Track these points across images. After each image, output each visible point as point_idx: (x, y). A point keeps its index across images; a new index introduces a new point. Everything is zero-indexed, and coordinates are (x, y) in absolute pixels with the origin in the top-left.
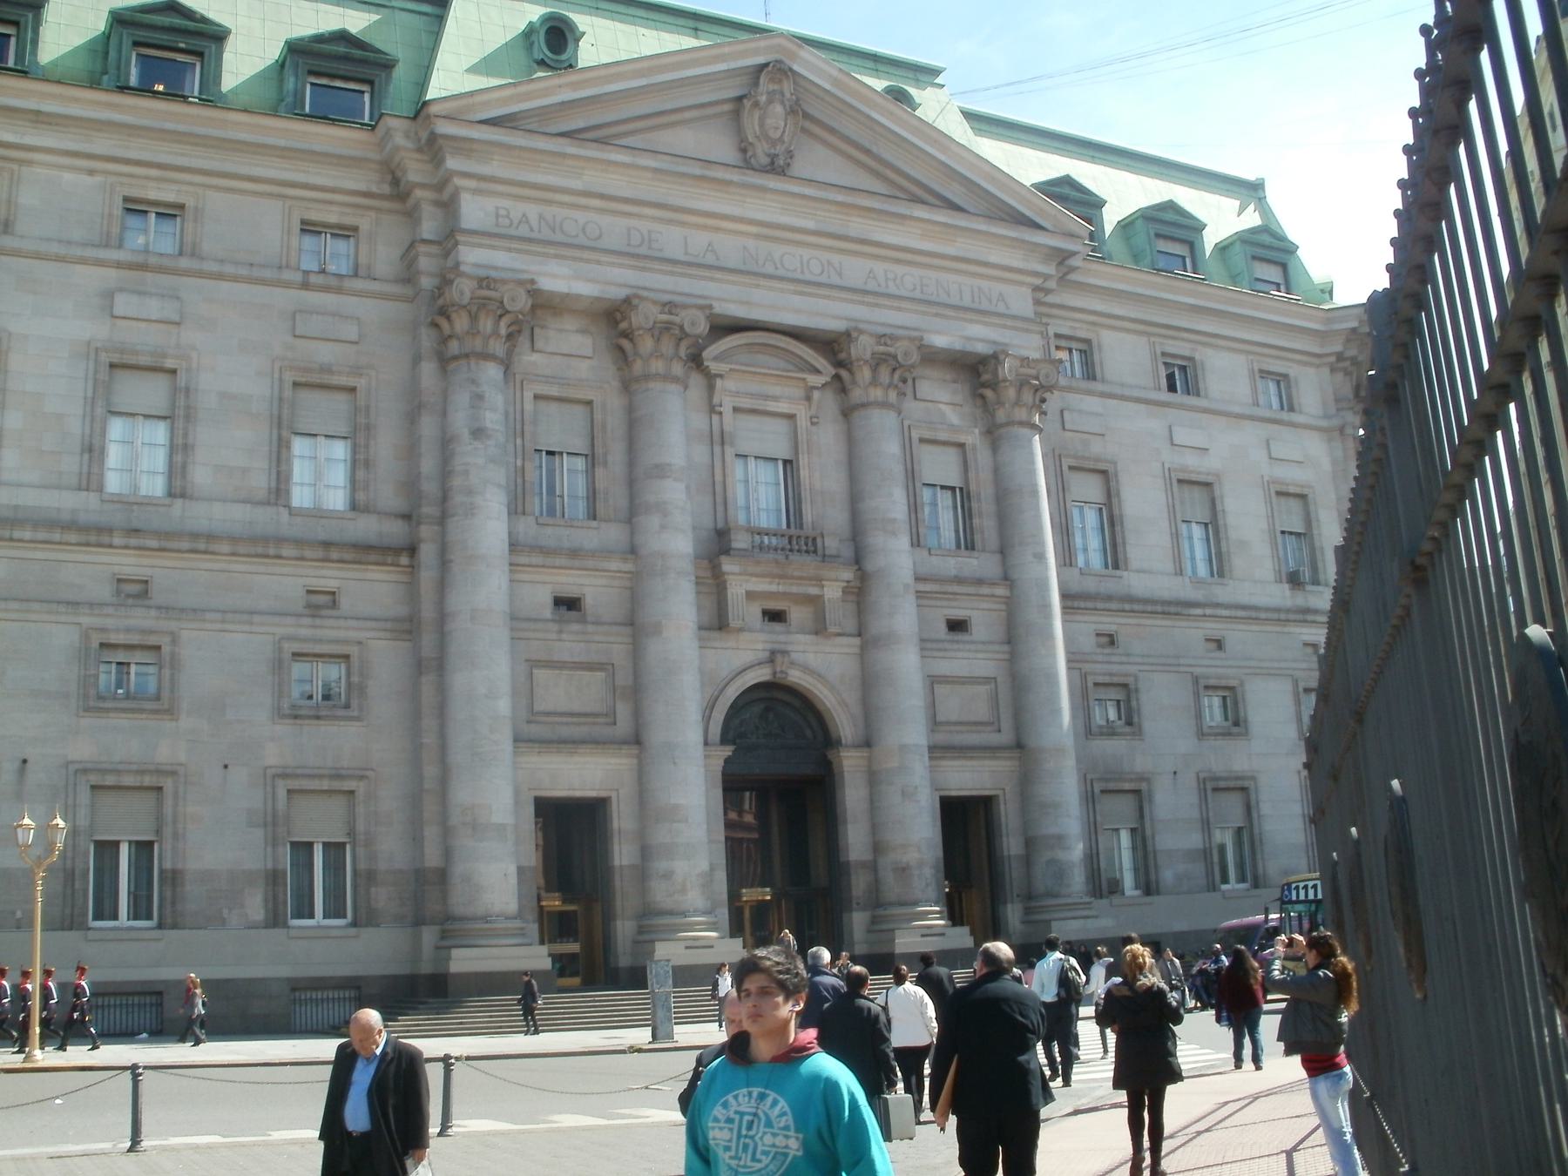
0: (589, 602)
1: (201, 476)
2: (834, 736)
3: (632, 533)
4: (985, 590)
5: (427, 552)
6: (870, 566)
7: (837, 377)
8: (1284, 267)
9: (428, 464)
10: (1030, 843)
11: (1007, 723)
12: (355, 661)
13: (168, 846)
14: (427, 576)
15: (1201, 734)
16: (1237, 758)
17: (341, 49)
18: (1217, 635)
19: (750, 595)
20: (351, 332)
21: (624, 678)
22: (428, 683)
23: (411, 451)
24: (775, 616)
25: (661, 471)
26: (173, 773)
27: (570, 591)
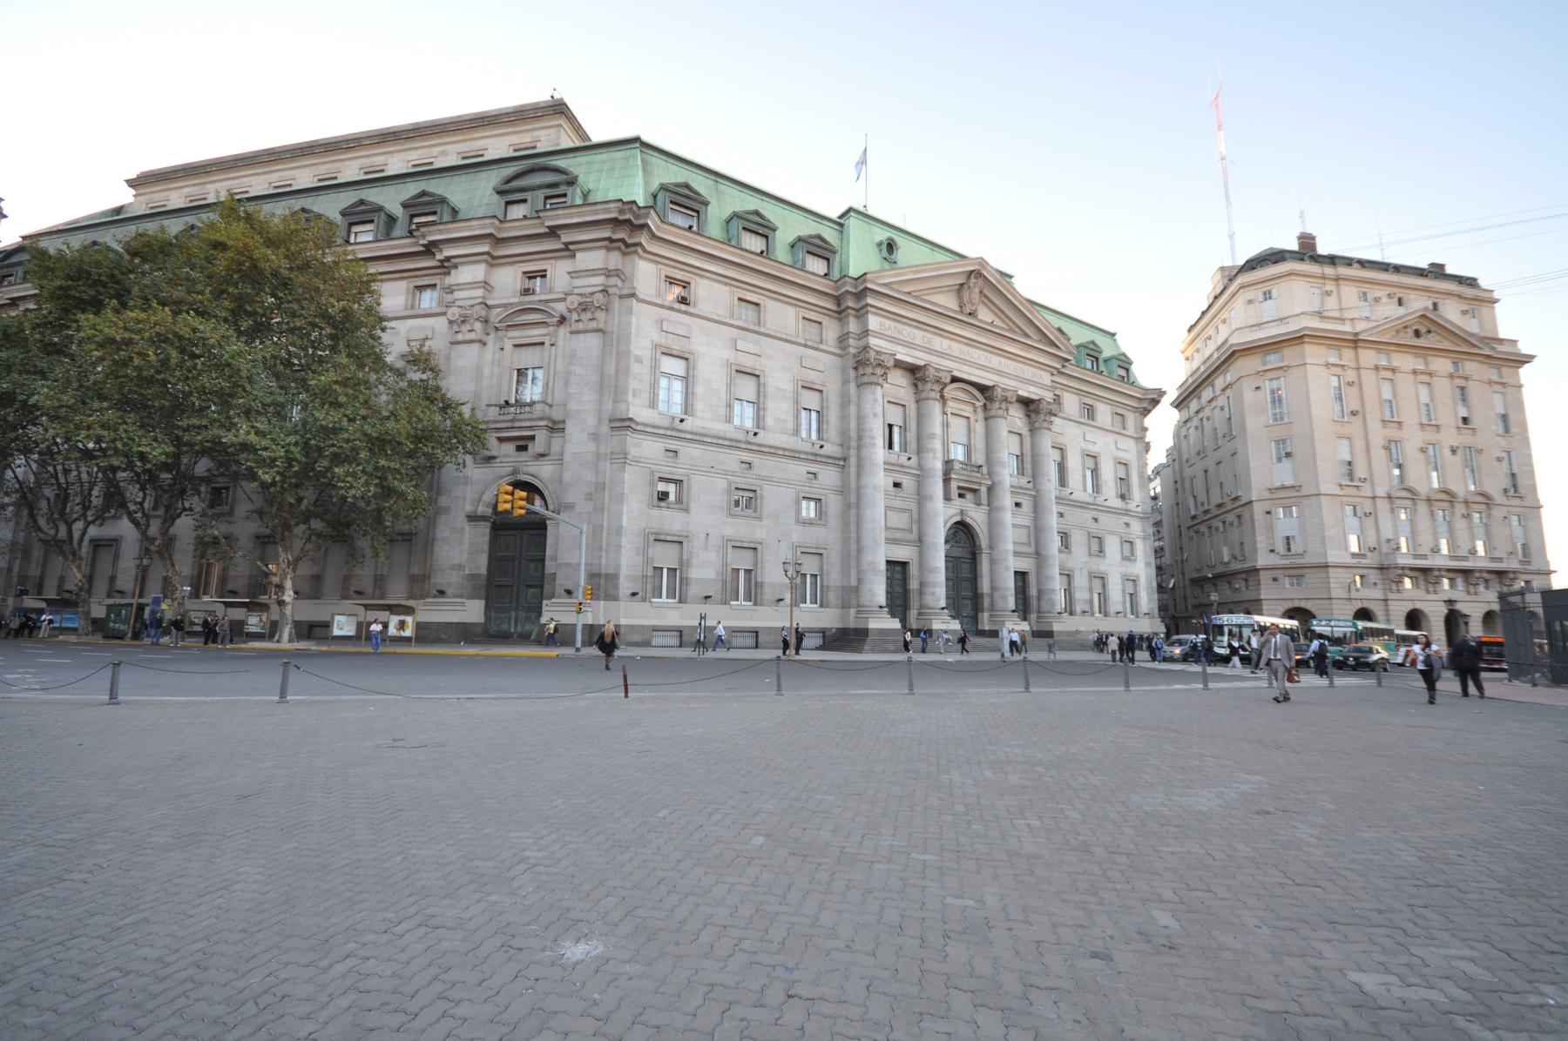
0: (904, 485)
1: (769, 421)
2: (977, 543)
4: (1029, 492)
5: (853, 460)
6: (996, 479)
7: (985, 405)
8: (1127, 370)
9: (853, 425)
10: (1040, 592)
11: (1033, 544)
12: (823, 501)
13: (759, 571)
14: (853, 470)
15: (1090, 555)
16: (1102, 566)
17: (818, 242)
18: (1096, 516)
19: (959, 488)
20: (821, 367)
21: (915, 516)
22: (853, 512)
23: (844, 418)
24: (961, 496)
25: (933, 436)
26: (761, 543)
27: (898, 481)
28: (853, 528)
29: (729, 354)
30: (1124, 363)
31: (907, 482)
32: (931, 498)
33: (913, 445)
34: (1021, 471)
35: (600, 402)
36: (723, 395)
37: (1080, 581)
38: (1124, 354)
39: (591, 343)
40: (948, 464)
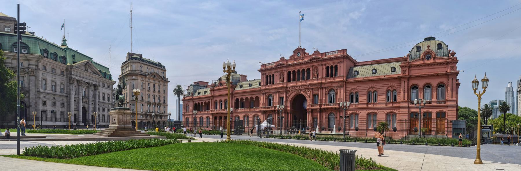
3: (78, 96)
5: (69, 97)
6: (90, 99)
9: (69, 91)
16: (104, 113)
17: (64, 57)
20: (64, 80)
21: (77, 106)
25: (80, 92)
28: (69, 109)
29: (51, 79)
30: (110, 76)
31: (76, 101)
32: (80, 103)
33: (77, 94)
34: (93, 97)
35: (35, 88)
36: (51, 86)
37: (101, 116)
38: (110, 74)
39: (33, 78)
40: (82, 97)
